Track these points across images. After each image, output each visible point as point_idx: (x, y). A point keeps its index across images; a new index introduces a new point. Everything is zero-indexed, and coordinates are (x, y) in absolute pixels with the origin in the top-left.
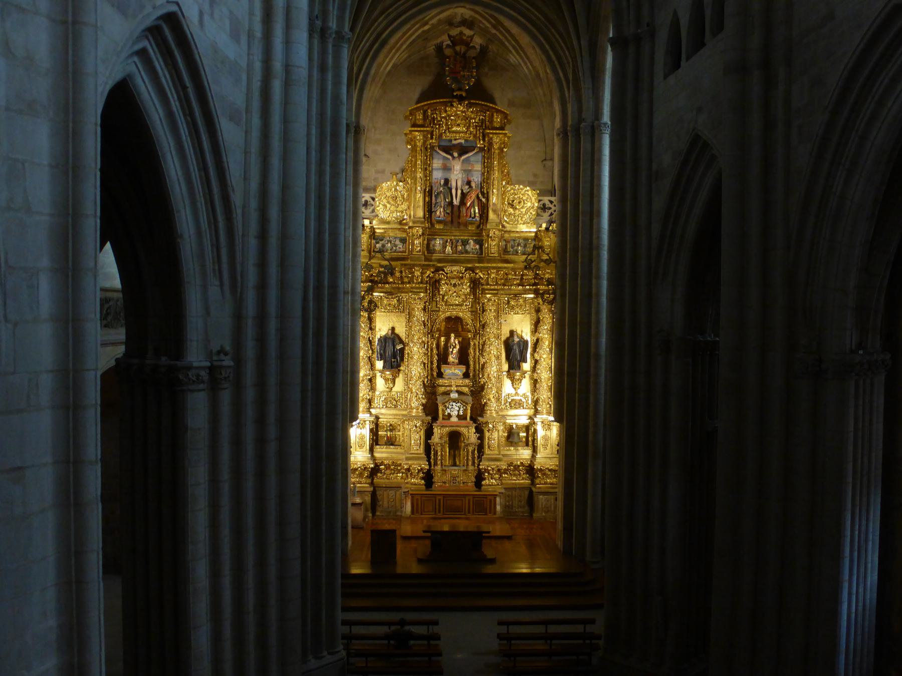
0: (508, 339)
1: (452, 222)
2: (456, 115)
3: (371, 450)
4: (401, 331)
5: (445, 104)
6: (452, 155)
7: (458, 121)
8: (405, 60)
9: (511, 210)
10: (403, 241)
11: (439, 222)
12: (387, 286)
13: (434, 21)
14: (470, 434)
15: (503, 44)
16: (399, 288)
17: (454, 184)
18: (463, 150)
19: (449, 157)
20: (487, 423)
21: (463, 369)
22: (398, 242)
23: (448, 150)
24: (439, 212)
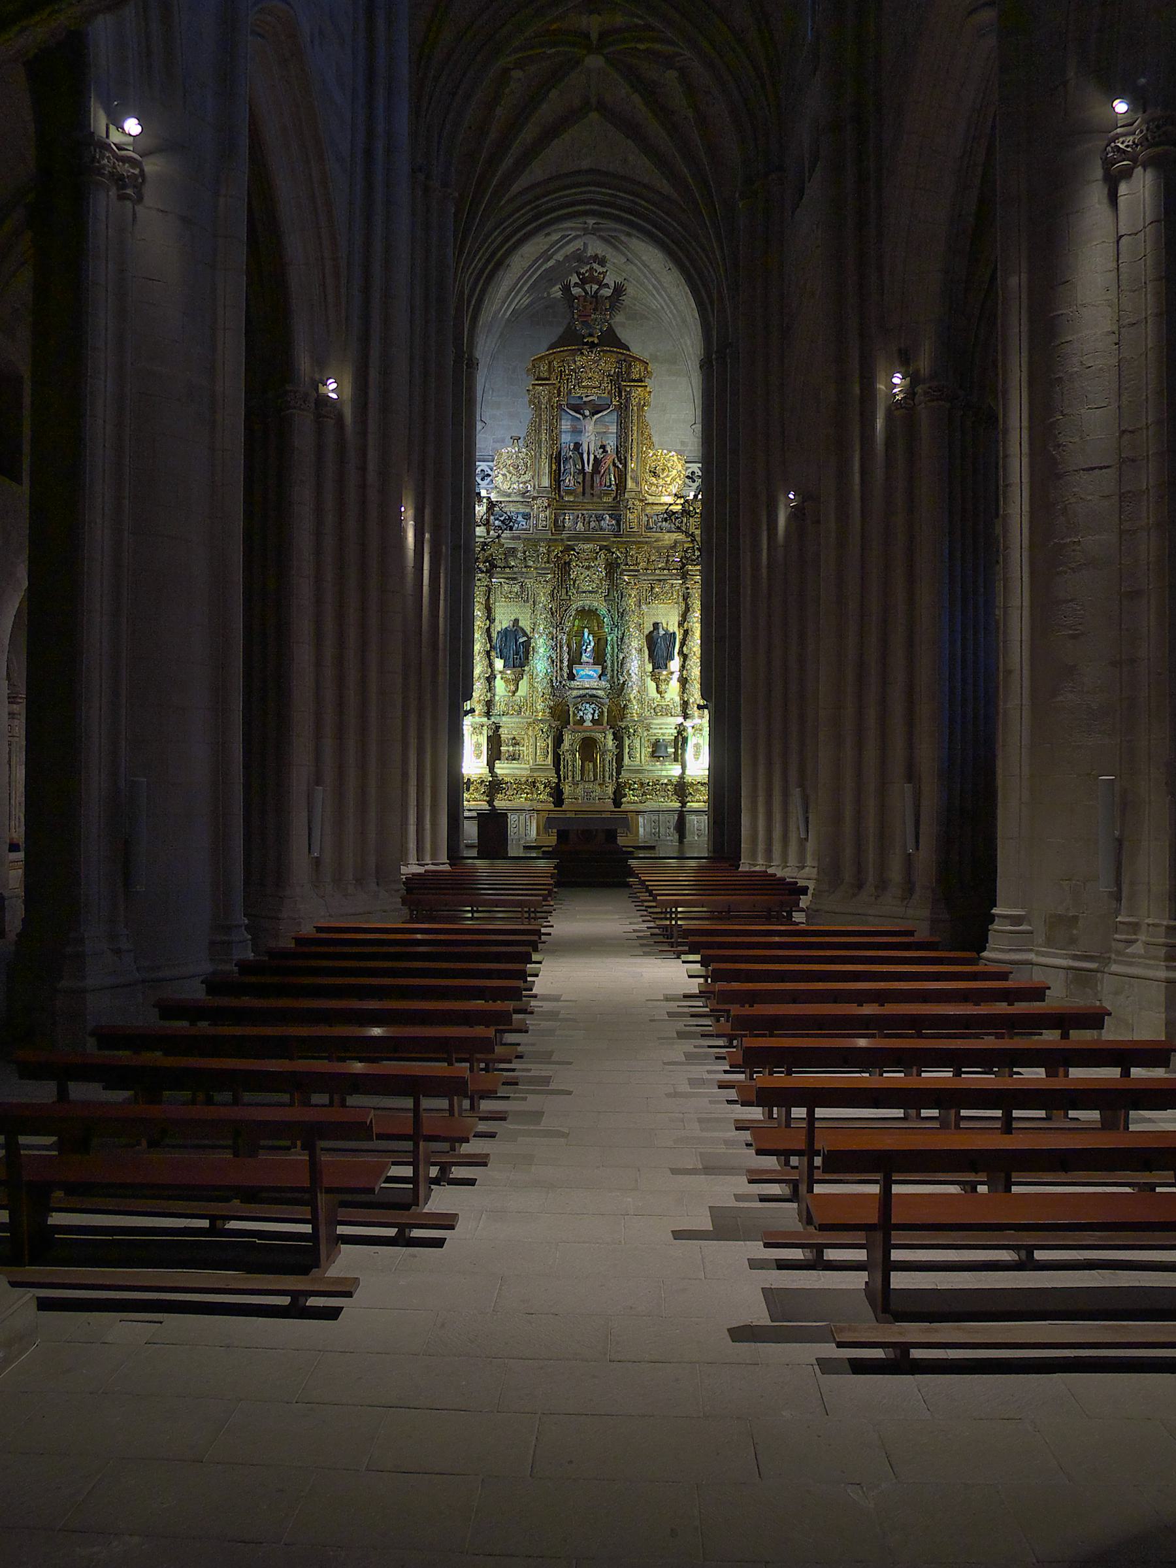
1: (584, 494)
3: (491, 765)
4: (525, 624)
6: (583, 415)
10: (527, 516)
11: (569, 493)
12: (507, 570)
13: (559, 256)
20: (627, 728)
21: (599, 669)
22: (520, 518)
24: (569, 481)
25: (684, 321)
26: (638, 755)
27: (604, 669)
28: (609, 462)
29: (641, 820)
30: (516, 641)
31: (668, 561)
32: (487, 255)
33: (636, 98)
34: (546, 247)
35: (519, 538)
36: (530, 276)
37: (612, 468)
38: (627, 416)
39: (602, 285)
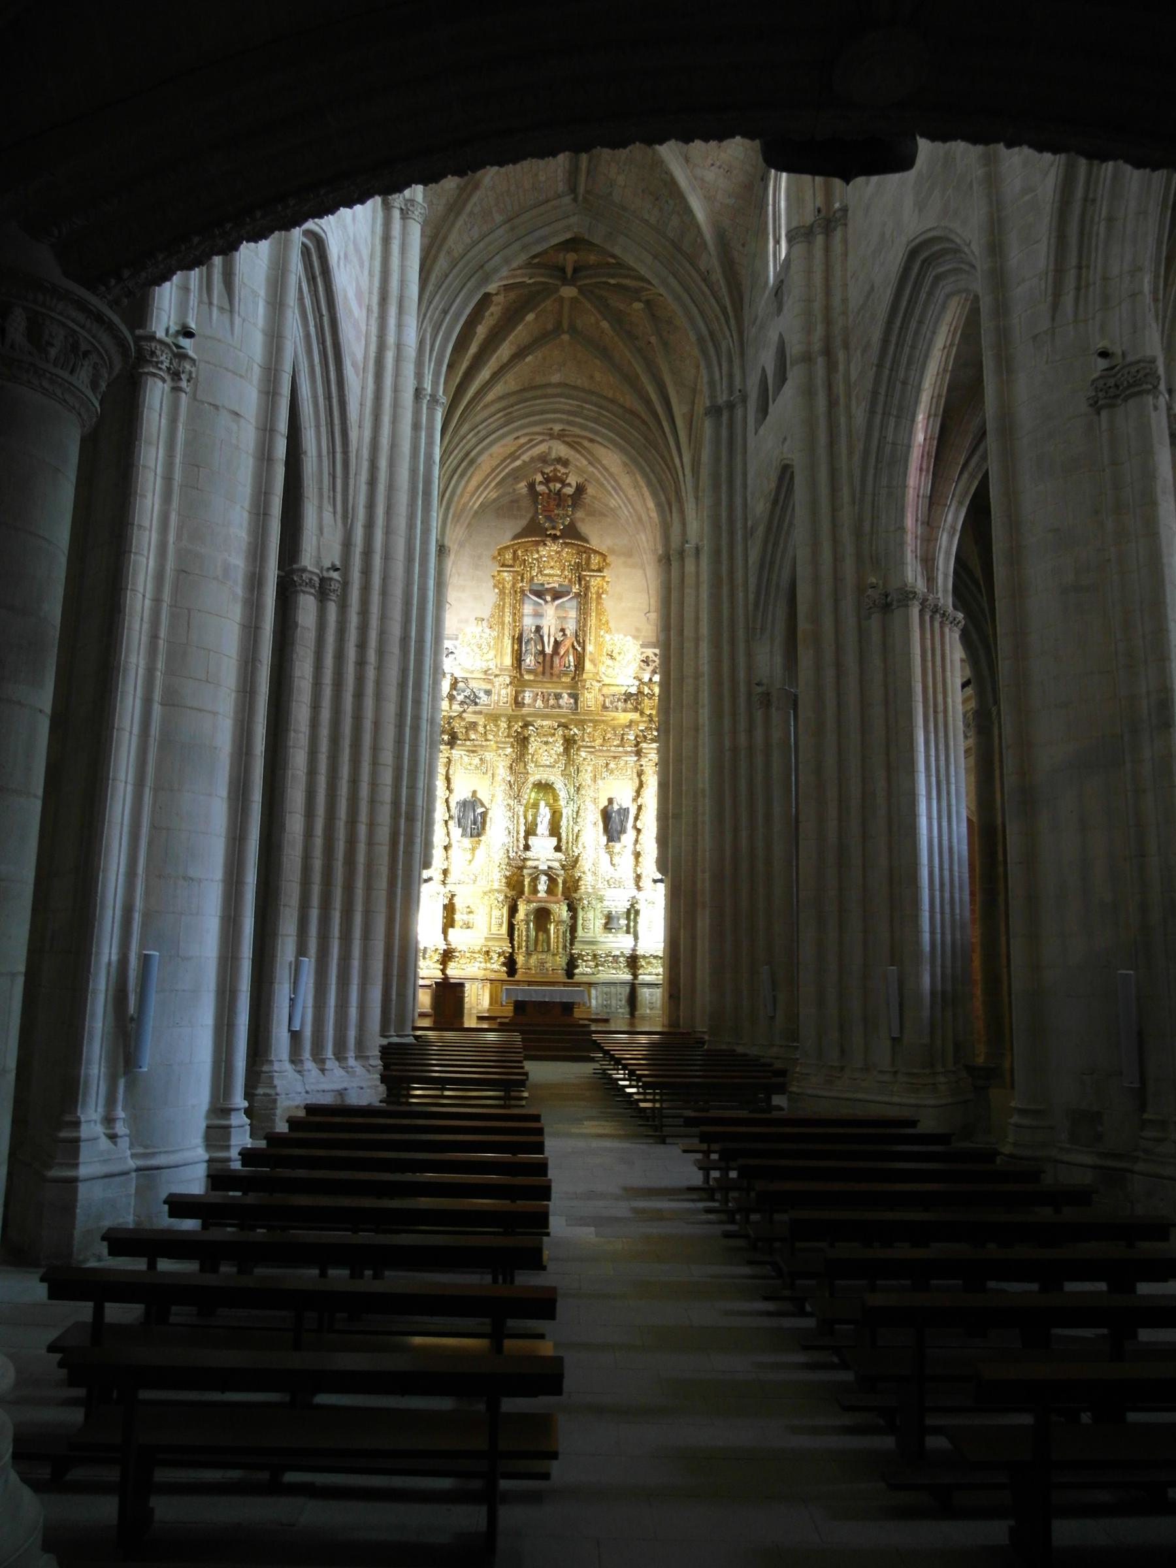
0: (606, 807)
1: (544, 673)
2: (550, 556)
3: (445, 932)
5: (537, 543)
7: (551, 563)
8: (494, 500)
9: (609, 662)
10: (488, 693)
11: (529, 672)
12: (468, 743)
13: (526, 457)
14: (561, 911)
15: (602, 485)
16: (482, 746)
17: (545, 631)
18: (557, 595)
19: (541, 601)
20: (581, 899)
21: (554, 841)
22: (482, 694)
23: (539, 594)
24: (529, 661)
25: (640, 519)
26: (591, 924)
27: (560, 840)
28: (568, 643)
29: (593, 992)
30: (474, 811)
31: (622, 739)
32: (464, 451)
33: (605, 325)
34: (513, 449)
35: (480, 713)
36: (498, 475)
37: (571, 650)
38: (586, 603)
39: (564, 484)
